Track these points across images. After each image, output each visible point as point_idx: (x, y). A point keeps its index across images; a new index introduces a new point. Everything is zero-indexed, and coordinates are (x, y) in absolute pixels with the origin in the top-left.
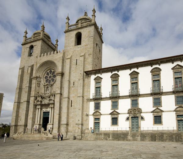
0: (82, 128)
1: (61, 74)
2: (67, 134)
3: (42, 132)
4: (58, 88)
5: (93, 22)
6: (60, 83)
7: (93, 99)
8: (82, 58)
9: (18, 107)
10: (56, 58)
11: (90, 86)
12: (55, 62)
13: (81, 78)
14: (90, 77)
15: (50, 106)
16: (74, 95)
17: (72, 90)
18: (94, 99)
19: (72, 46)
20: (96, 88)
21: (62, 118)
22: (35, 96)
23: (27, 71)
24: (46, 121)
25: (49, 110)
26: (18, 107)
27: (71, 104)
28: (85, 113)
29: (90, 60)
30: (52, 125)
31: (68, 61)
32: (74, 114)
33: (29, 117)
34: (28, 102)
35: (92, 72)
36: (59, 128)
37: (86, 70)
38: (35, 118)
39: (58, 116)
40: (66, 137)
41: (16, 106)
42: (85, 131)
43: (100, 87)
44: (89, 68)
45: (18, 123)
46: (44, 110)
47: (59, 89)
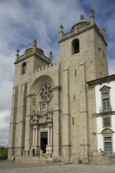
0: (88, 150)
1: (58, 89)
2: (70, 157)
3: (40, 154)
4: (56, 104)
5: (92, 24)
6: (57, 98)
7: (101, 114)
8: (82, 68)
9: (14, 128)
10: (52, 71)
11: (95, 99)
12: (51, 76)
13: (82, 90)
14: (94, 87)
15: (48, 125)
16: (76, 111)
17: (73, 105)
18: (102, 114)
19: (69, 56)
20: (103, 100)
21: (63, 138)
22: (30, 116)
23: (22, 89)
24: (44, 142)
25: (47, 129)
26: (14, 128)
27: (72, 122)
28: (91, 131)
29: (92, 68)
30: (51, 147)
31: (65, 73)
32: (76, 133)
33: (26, 139)
34: (24, 122)
35: (96, 81)
36: (60, 150)
37: (88, 80)
38: (32, 140)
39: (58, 136)
40: (69, 161)
41: (12, 127)
42: (93, 154)
43: (108, 98)
44: (92, 77)
45: (14, 145)
46: (42, 130)
47: (57, 106)
